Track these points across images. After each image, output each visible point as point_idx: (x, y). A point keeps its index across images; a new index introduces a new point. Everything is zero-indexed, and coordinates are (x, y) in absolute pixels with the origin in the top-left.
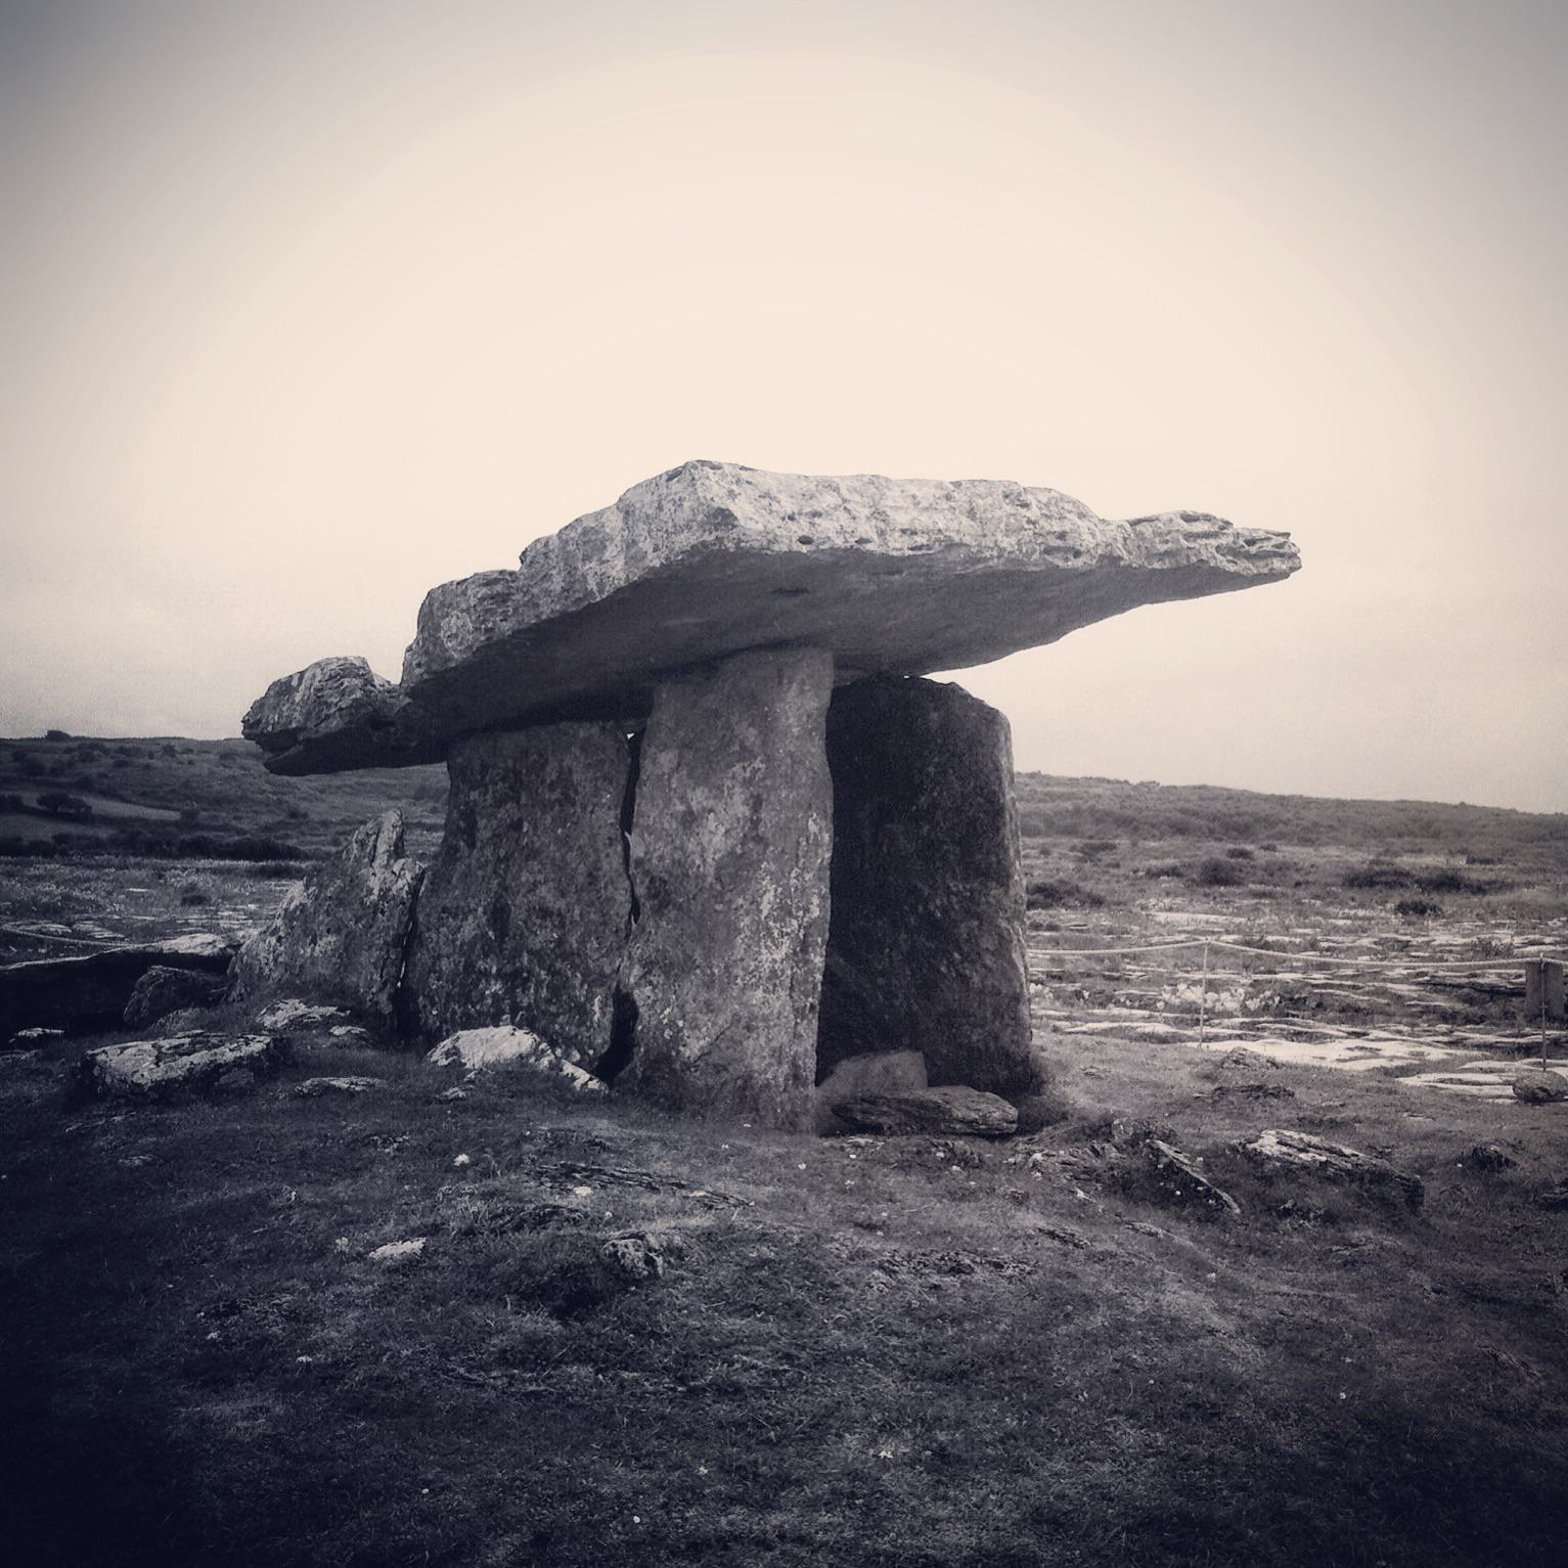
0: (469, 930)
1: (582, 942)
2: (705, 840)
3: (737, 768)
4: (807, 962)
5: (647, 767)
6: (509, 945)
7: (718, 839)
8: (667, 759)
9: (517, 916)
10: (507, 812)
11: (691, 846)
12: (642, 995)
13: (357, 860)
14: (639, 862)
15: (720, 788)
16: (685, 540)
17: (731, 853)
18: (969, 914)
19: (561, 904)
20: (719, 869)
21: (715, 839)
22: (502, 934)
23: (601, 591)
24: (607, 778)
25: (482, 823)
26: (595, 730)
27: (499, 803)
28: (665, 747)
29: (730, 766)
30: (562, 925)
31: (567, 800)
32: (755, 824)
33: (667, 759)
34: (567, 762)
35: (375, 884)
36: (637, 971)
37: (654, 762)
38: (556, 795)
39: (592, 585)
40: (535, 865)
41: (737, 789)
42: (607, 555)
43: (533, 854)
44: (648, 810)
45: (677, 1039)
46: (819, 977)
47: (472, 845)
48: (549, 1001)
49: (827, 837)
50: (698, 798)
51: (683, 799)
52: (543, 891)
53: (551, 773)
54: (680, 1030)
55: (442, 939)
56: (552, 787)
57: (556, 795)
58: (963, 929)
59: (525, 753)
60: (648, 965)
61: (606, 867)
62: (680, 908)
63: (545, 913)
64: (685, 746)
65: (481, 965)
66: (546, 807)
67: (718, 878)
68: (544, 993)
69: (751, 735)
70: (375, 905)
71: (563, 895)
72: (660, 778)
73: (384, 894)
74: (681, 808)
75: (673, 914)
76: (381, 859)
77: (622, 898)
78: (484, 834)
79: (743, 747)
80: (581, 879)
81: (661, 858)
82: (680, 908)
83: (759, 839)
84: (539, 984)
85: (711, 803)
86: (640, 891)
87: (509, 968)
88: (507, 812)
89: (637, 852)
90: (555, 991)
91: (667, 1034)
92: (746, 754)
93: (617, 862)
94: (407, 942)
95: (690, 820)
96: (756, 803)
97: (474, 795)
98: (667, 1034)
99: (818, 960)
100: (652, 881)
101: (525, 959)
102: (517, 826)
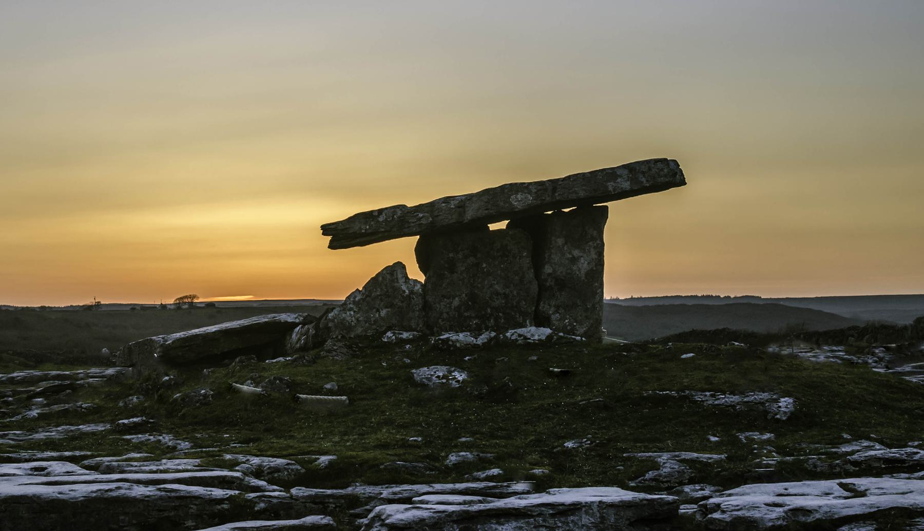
2: (580, 266)
3: (591, 243)
7: (585, 265)
8: (560, 241)
10: (471, 260)
11: (575, 268)
14: (549, 274)
17: (592, 270)
23: (614, 190)
33: (560, 241)
36: (553, 309)
39: (610, 188)
42: (619, 180)
50: (576, 253)
51: (570, 253)
55: (442, 307)
60: (557, 308)
63: (498, 294)
65: (466, 314)
69: (595, 233)
70: (409, 296)
73: (412, 292)
77: (535, 288)
88: (471, 260)
89: (548, 269)
93: (531, 274)
95: (574, 260)
97: (451, 255)
101: (489, 310)
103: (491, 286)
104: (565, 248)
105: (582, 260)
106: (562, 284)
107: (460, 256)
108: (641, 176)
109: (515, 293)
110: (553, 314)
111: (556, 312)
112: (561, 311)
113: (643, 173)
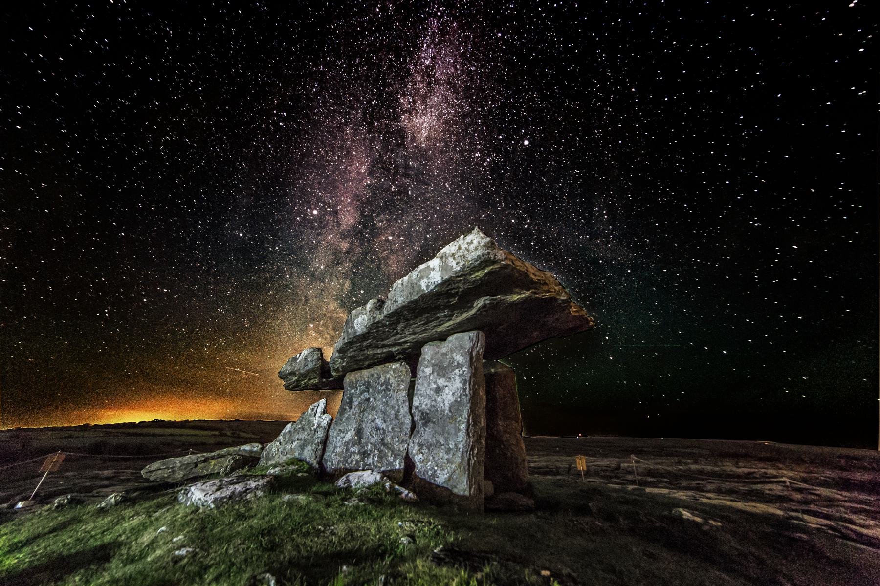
0: (348, 436)
1: (392, 438)
3: (457, 371)
4: (481, 443)
5: (420, 374)
6: (363, 441)
9: (367, 432)
11: (439, 399)
12: (418, 458)
13: (310, 415)
14: (417, 407)
15: (450, 378)
16: (474, 255)
17: (456, 401)
18: (505, 432)
19: (384, 426)
20: (450, 408)
21: (448, 397)
22: (360, 438)
23: (428, 287)
24: (402, 381)
25: (355, 400)
26: (398, 365)
27: (362, 393)
28: (427, 367)
29: (453, 370)
30: (384, 433)
31: (387, 389)
32: (465, 390)
33: (428, 370)
34: (388, 376)
35: (316, 422)
37: (423, 371)
38: (384, 387)
39: (424, 287)
40: (374, 412)
41: (457, 378)
42: (432, 273)
43: (373, 408)
44: (422, 387)
45: (434, 475)
46: (484, 449)
47: (351, 408)
48: (378, 462)
49: (484, 397)
50: (441, 382)
51: (435, 383)
52: (377, 421)
53: (382, 380)
54: (436, 471)
56: (382, 385)
57: (384, 387)
58: (504, 438)
59: (372, 375)
60: (421, 445)
61: (402, 410)
62: (434, 423)
63: (378, 429)
64: (433, 365)
65: (352, 450)
66: (379, 392)
67: (450, 411)
68: (376, 459)
71: (385, 422)
72: (426, 377)
73: (319, 426)
74: (435, 386)
75: (431, 425)
76: (318, 414)
77: (408, 421)
78: (356, 403)
79: (458, 363)
80: (392, 416)
81: (426, 405)
82: (434, 423)
83: (466, 395)
84: (374, 455)
85: (446, 384)
86: (416, 418)
87: (362, 450)
89: (416, 403)
90: (381, 457)
91: (430, 473)
92: (459, 366)
93: (406, 409)
94: (325, 442)
95: (438, 390)
96: (464, 384)
97: (353, 391)
98: (430, 473)
99: (484, 443)
100: (422, 414)
102: (368, 400)
103: (373, 421)
104: (431, 378)
105: (447, 390)
106: (426, 418)
107: (358, 391)
108: (451, 259)
109: (390, 429)
110: (417, 454)
111: (420, 451)
112: (425, 451)
113: (453, 255)
